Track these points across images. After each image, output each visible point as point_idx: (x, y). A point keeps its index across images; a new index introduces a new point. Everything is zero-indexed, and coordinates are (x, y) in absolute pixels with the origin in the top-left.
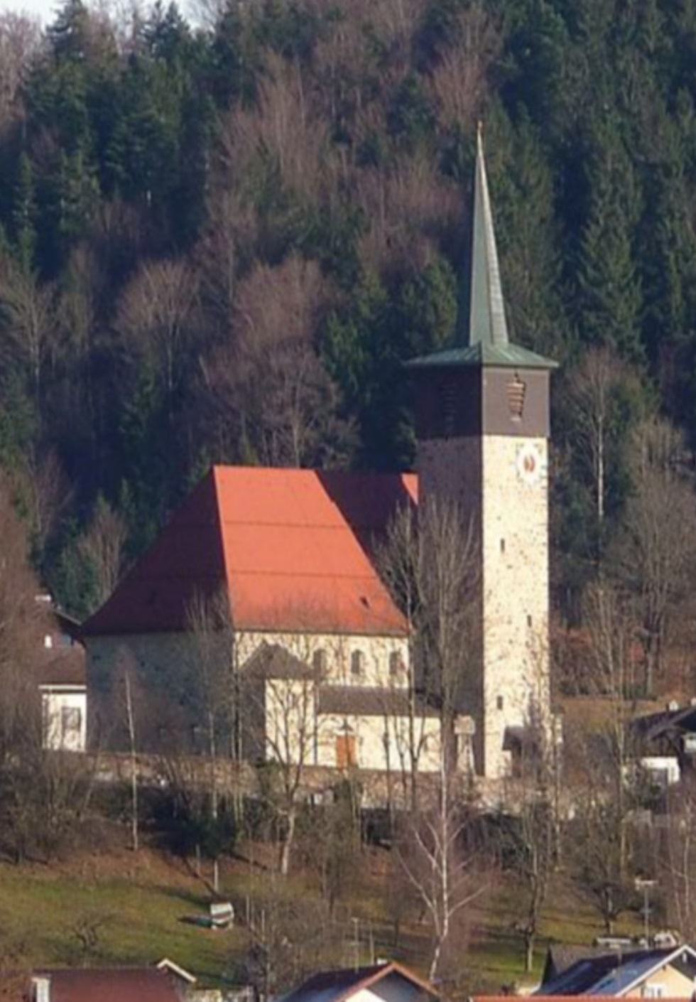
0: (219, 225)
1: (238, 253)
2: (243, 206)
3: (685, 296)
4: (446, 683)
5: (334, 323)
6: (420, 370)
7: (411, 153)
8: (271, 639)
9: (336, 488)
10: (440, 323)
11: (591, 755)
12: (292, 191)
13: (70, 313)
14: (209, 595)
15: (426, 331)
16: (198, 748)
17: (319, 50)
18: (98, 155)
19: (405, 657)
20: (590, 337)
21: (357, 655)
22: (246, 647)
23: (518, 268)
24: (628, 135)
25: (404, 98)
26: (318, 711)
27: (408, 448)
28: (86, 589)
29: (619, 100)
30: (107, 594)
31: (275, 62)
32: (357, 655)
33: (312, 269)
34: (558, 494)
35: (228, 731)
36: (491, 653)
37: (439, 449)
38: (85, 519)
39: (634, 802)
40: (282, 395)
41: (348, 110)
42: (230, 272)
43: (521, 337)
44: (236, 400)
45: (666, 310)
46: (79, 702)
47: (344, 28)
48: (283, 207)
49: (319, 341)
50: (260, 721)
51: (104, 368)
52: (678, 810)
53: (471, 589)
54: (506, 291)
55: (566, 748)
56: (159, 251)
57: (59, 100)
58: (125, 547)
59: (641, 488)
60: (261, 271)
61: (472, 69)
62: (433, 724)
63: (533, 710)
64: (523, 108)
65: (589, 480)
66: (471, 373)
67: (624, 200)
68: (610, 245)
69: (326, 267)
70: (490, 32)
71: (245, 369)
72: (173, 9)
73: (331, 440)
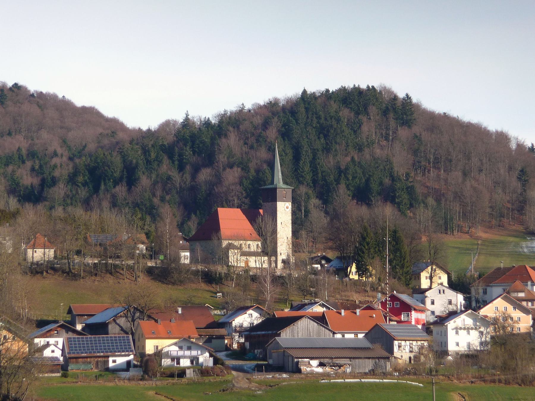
0: (219, 161)
1: (223, 166)
2: (224, 157)
3: (322, 175)
4: (269, 249)
5: (244, 180)
6: (263, 189)
7: (261, 147)
8: (230, 242)
9: (244, 212)
10: (268, 180)
11: (300, 264)
12: (235, 154)
13: (186, 178)
14: (217, 233)
15: (264, 182)
16: (214, 263)
17: (241, 127)
18: (192, 147)
19: (260, 245)
20: (301, 183)
21: (249, 245)
22: (225, 243)
23: (285, 169)
24: (309, 143)
25: (260, 136)
26: (241, 256)
27: (260, 204)
28: (189, 232)
29: (307, 136)
30: (194, 233)
31: (231, 129)
32: (249, 245)
33: (239, 169)
34: (294, 213)
35: (221, 259)
36: (279, 244)
37: (269, 205)
38: (189, 218)
39: (310, 273)
40: (233, 194)
41: (247, 138)
42: (221, 170)
43: (285, 182)
44: (222, 195)
45: (317, 177)
46: (188, 254)
47: (246, 122)
48: (233, 157)
49: (241, 183)
50: (228, 258)
51: (193, 189)
52: (320, 275)
53: (274, 232)
54: (282, 174)
55: (295, 262)
56: (205, 166)
57: (183, 136)
58: (198, 224)
59: (312, 212)
60: (228, 170)
61: (275, 130)
62: (266, 258)
63: (288, 255)
64: (286, 138)
65: (301, 210)
66: (275, 189)
67: (308, 156)
68: (305, 165)
69: (242, 169)
70: (279, 123)
71: (224, 189)
72: (209, 119)
73: (244, 203)
